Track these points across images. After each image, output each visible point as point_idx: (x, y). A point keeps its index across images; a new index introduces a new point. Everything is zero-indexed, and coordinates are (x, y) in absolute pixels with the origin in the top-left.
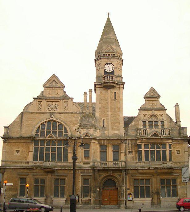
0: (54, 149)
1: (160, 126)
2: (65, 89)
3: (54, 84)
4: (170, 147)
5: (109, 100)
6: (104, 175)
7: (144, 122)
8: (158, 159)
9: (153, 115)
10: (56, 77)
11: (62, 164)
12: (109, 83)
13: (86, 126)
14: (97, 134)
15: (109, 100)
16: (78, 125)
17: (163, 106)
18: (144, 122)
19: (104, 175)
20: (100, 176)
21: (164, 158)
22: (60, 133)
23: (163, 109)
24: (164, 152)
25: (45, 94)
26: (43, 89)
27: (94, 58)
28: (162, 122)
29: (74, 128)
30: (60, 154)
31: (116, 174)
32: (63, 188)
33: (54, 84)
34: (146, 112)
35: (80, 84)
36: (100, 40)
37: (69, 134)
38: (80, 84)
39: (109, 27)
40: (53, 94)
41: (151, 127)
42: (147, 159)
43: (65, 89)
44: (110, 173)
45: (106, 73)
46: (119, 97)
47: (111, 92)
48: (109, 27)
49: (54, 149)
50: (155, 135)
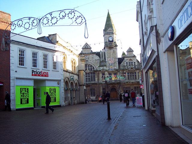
0: (89, 76)
1: (133, 65)
2: (92, 49)
3: (87, 47)
4: (138, 73)
5: (111, 53)
6: (111, 86)
7: (127, 63)
8: (133, 79)
9: (130, 60)
10: (88, 44)
11: (93, 82)
12: (110, 45)
13: (103, 66)
14: (107, 69)
15: (111, 53)
16: (99, 65)
17: (135, 55)
18: (127, 63)
19: (111, 86)
20: (109, 86)
21: (136, 78)
22: (91, 69)
23: (134, 56)
24: (136, 76)
25: (83, 52)
26: (82, 50)
27: (103, 34)
28: (135, 63)
29: (97, 67)
30: (92, 78)
31: (116, 85)
32: (94, 93)
33: (87, 47)
34: (127, 58)
35: (98, 46)
36: (106, 25)
37: (95, 69)
38: (98, 46)
39: (109, 18)
40: (87, 51)
41: (130, 65)
42: (128, 79)
43: (92, 49)
44: (114, 85)
45: (109, 41)
46: (116, 52)
47: (112, 51)
48: (109, 18)
49: (89, 76)
50: (132, 68)
